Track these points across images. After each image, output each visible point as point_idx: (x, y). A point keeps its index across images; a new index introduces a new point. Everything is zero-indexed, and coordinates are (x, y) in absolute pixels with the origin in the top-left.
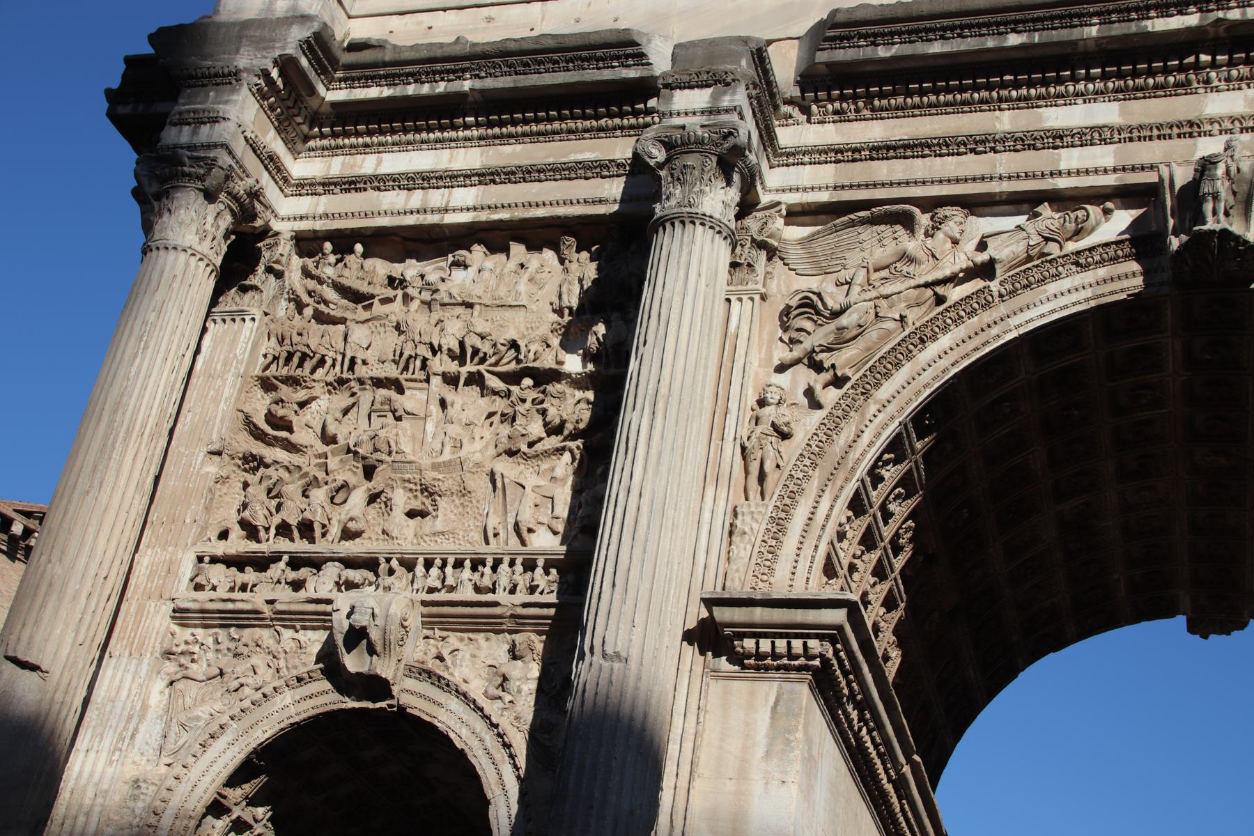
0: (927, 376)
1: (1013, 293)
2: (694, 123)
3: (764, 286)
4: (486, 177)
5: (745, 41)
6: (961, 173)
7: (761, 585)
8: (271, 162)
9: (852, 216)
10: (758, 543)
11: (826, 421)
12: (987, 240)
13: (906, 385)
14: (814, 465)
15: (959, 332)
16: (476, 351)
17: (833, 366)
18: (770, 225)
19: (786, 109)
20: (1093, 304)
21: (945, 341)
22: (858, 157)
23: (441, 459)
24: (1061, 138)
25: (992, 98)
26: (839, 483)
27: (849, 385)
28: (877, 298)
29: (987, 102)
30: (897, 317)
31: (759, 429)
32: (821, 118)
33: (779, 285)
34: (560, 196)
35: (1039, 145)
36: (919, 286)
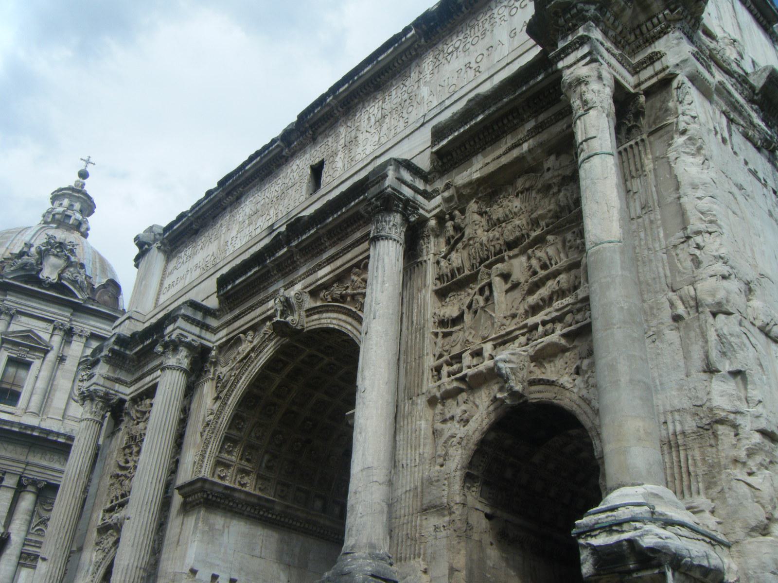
1: (257, 356)
8: (117, 380)
14: (213, 433)
21: (243, 378)
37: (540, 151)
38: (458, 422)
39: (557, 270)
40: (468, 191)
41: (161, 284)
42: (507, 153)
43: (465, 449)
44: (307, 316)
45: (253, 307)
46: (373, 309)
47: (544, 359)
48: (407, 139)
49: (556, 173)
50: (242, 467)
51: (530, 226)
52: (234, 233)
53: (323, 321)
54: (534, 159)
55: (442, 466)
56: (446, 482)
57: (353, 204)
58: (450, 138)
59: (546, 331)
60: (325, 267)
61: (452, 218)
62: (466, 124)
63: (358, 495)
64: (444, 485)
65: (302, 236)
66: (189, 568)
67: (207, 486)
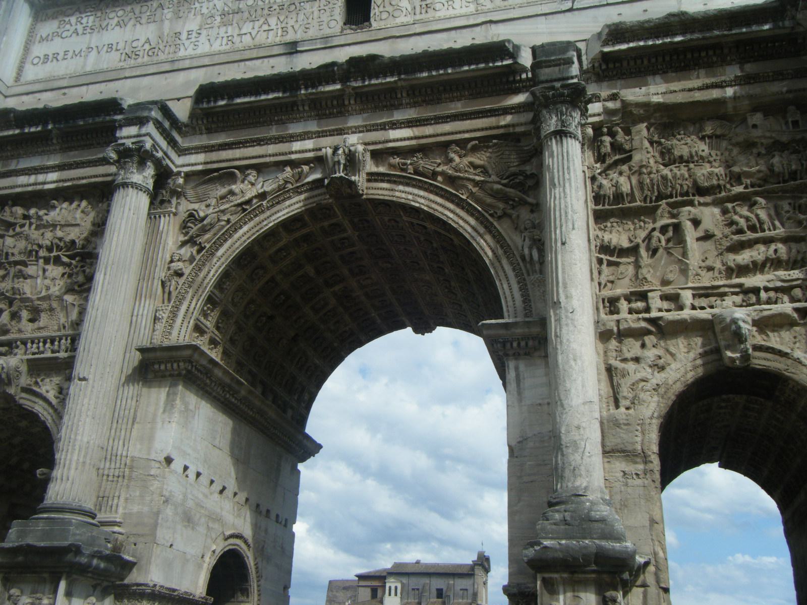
0: (237, 244)
1: (273, 206)
2: (129, 143)
3: (176, 208)
4: (61, 168)
5: (154, 103)
6: (254, 154)
7: (165, 340)
10: (164, 322)
15: (251, 224)
16: (58, 246)
20: (303, 208)
21: (245, 228)
23: (40, 296)
26: (200, 294)
27: (204, 251)
31: (169, 272)
34: (92, 174)
36: (235, 206)
37: (747, 102)
38: (650, 366)
39: (772, 237)
40: (642, 112)
41: (27, 49)
42: (703, 89)
43: (662, 397)
44: (369, 181)
45: (263, 140)
46: (570, 217)
47: (766, 326)
48: (543, 17)
49: (768, 134)
50: (214, 336)
51: (728, 179)
52: (193, 24)
53: (397, 194)
54: (735, 108)
55: (627, 408)
56: (639, 428)
57: (466, 68)
58: (632, 45)
59: (769, 298)
60: (401, 128)
61: (612, 134)
62: (657, 37)
63: (582, 431)
64: (637, 430)
65: (370, 79)
66: (165, 455)
67: (196, 356)
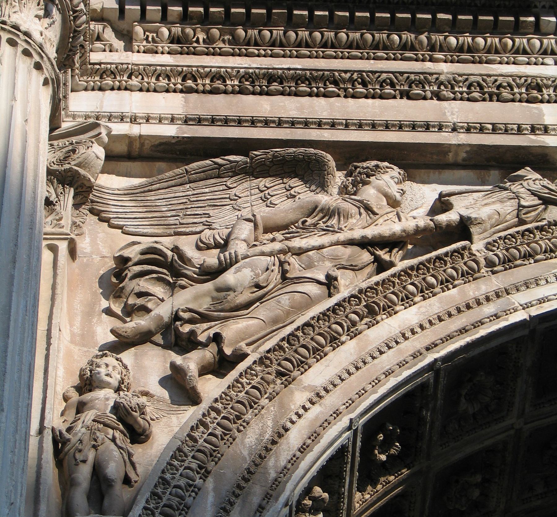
9: (218, 160)
11: (219, 406)
12: (452, 199)
13: (353, 370)
17: (217, 338)
18: (82, 149)
19: (95, 27)
22: (222, 87)
24: (540, 90)
25: (421, 43)
28: (283, 252)
29: (413, 48)
30: (322, 278)
31: (89, 416)
32: (149, 46)
33: (94, 242)
35: (506, 94)
36: (351, 243)
